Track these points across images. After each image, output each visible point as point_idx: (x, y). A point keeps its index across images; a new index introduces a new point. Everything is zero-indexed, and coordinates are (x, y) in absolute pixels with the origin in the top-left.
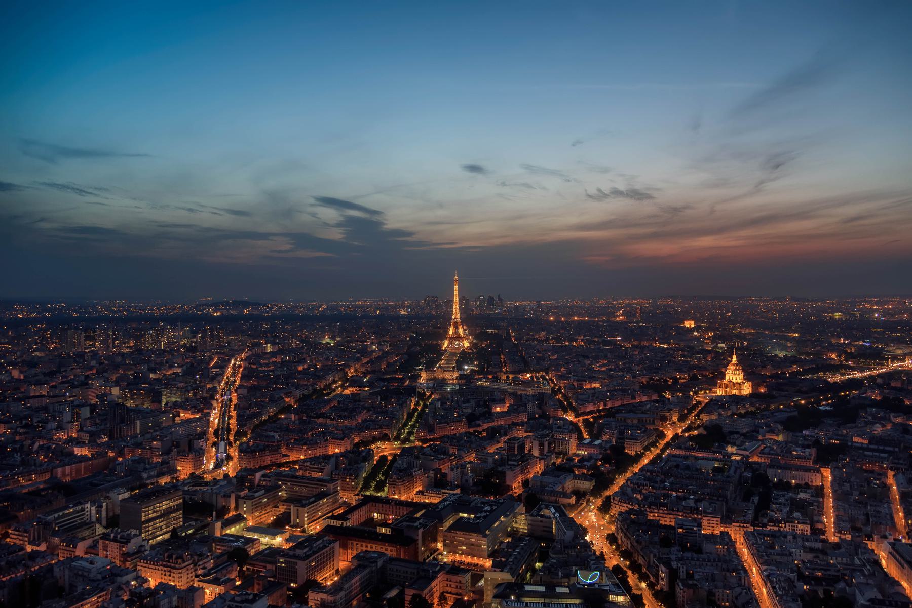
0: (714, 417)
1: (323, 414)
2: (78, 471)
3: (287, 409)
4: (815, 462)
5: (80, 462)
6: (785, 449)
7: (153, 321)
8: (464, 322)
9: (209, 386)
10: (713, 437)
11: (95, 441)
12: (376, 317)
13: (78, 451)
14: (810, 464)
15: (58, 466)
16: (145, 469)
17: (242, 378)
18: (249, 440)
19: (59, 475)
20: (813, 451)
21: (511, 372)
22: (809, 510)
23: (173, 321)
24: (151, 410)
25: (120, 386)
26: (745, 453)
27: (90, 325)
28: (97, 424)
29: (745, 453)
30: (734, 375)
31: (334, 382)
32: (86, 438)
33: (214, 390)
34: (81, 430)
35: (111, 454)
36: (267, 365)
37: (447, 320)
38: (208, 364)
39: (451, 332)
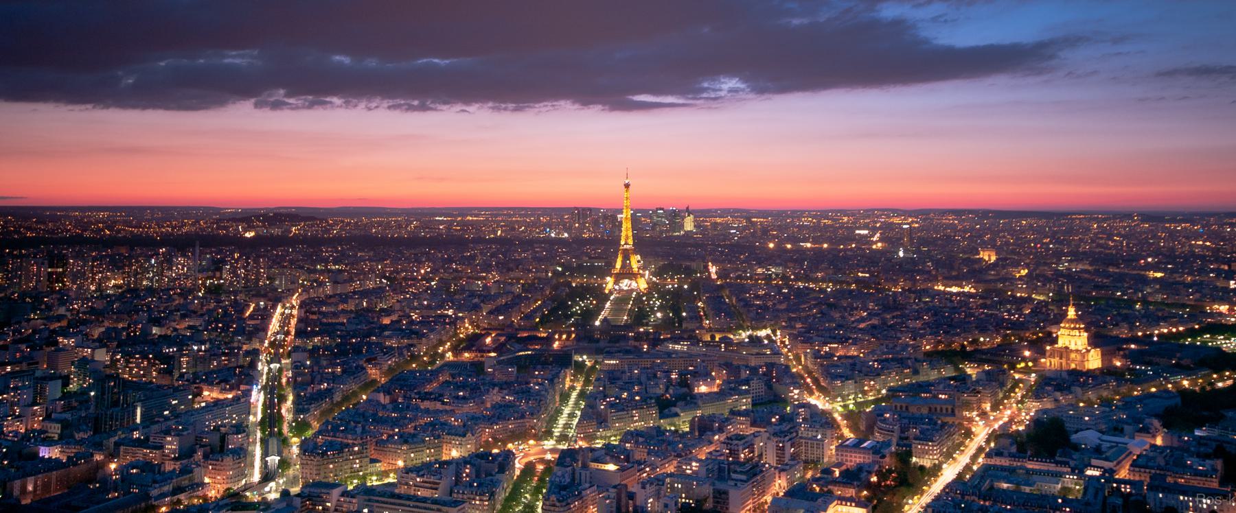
0: (1049, 406)
1: (431, 393)
2: (46, 486)
3: (370, 384)
4: (1221, 484)
5: (50, 470)
6: (1173, 458)
7: (148, 244)
9: (245, 347)
10: (1048, 439)
11: (72, 436)
12: (496, 240)
13: (45, 452)
14: (1214, 484)
15: (15, 478)
16: (155, 482)
17: (299, 333)
18: (316, 435)
19: (16, 492)
20: (1219, 464)
21: (719, 331)
23: (181, 244)
24: (160, 387)
25: (107, 347)
26: (1107, 465)
28: (73, 408)
29: (1107, 465)
30: (1072, 339)
31: (442, 343)
32: (55, 430)
33: (255, 353)
34: (48, 417)
36: (335, 315)
37: (613, 242)
38: (243, 311)
39: (618, 265)
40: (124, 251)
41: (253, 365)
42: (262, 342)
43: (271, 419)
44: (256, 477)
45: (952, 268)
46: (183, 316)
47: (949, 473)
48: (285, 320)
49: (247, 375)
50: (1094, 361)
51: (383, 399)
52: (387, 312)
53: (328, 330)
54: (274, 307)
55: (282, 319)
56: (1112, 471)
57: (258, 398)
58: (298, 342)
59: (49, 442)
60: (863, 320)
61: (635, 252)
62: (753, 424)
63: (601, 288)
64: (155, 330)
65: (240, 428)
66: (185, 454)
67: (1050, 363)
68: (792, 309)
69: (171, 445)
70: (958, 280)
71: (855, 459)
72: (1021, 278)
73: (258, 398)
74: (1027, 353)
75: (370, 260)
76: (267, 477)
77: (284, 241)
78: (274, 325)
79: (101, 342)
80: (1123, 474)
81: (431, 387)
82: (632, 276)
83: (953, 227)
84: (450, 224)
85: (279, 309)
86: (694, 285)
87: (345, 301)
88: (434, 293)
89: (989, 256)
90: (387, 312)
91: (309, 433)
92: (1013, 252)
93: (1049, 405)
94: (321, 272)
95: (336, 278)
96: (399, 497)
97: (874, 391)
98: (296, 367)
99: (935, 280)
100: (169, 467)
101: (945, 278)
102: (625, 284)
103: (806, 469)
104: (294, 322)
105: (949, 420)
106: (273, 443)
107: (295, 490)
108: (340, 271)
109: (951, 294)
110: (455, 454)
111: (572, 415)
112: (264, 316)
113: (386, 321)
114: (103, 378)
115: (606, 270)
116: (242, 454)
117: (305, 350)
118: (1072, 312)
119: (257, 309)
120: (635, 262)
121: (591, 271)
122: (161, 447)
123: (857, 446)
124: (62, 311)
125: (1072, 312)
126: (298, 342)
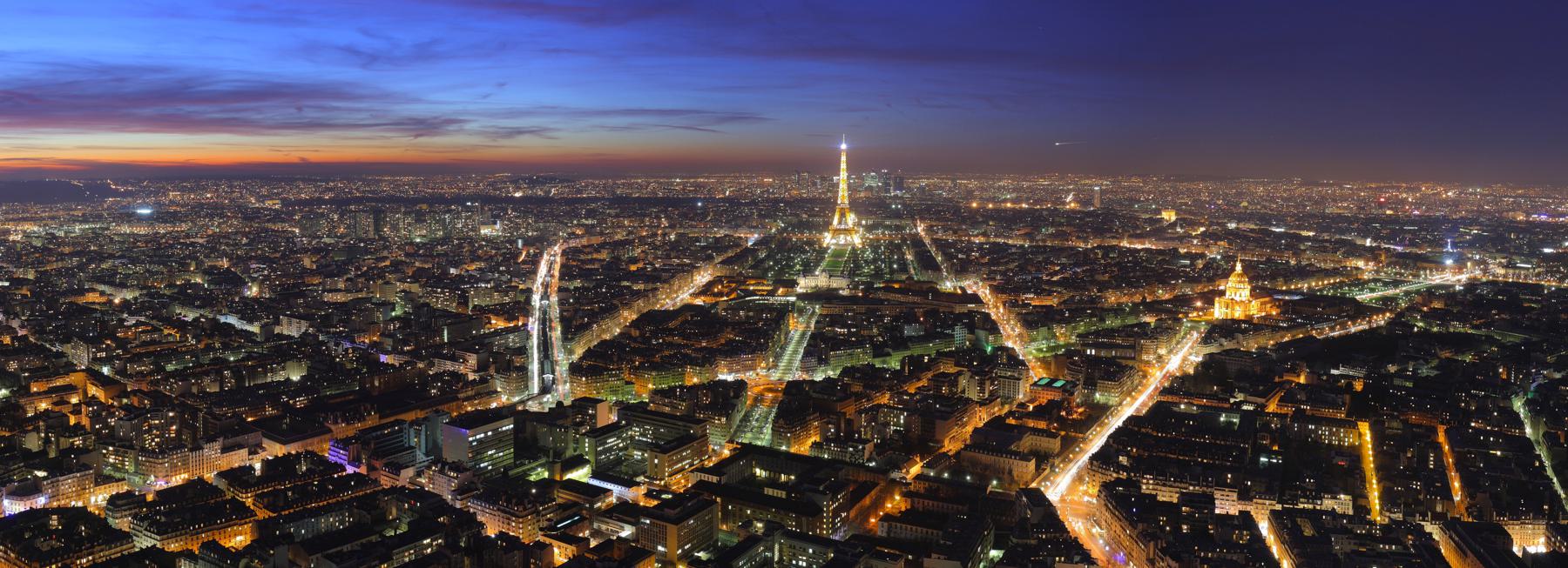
8: (855, 205)
17: (561, 278)
22: (1351, 480)
26: (1260, 400)
27: (380, 207)
33: (529, 291)
35: (421, 365)
36: (593, 261)
40: (424, 207)
41: (528, 301)
42: (534, 282)
43: (545, 346)
44: (536, 391)
45: (1137, 227)
46: (472, 261)
47: (1128, 411)
48: (551, 266)
49: (524, 308)
50: (1256, 309)
51: (635, 333)
52: (634, 260)
53: (586, 275)
54: (541, 254)
55: (549, 266)
56: (1264, 406)
57: (534, 326)
58: (565, 284)
59: (387, 353)
60: (1056, 273)
61: (851, 210)
62: (957, 365)
63: (819, 242)
64: (452, 271)
65: (523, 351)
66: (482, 367)
67: (1219, 312)
68: (993, 261)
69: (473, 360)
70: (1141, 237)
71: (1045, 397)
72: (1196, 237)
73: (534, 326)
74: (1199, 304)
75: (617, 216)
76: (545, 390)
77: (546, 200)
78: (543, 269)
79: (415, 278)
80: (1272, 407)
81: (671, 325)
82: (847, 231)
83: (1138, 190)
84: (684, 184)
85: (546, 257)
86: (904, 240)
87: (597, 251)
88: (674, 246)
89: (1169, 216)
90: (634, 260)
91: (575, 357)
92: (1191, 213)
93: (1213, 349)
94: (578, 226)
95: (589, 230)
96: (651, 412)
97: (1064, 336)
98: (561, 303)
99: (1121, 238)
100: (471, 377)
101: (1131, 236)
102: (842, 239)
103: (1003, 404)
104: (557, 267)
105: (1130, 363)
106: (547, 367)
107: (567, 402)
108: (593, 226)
109: (1138, 251)
110: (695, 380)
111: (795, 352)
112: (534, 261)
113: (633, 268)
114: (420, 307)
115: (826, 226)
116: (523, 370)
117: (567, 290)
118: (1239, 267)
119: (528, 254)
120: (851, 218)
121: (810, 226)
122: (465, 361)
123: (1049, 385)
124: (385, 253)
125: (1239, 267)
126: (565, 284)
